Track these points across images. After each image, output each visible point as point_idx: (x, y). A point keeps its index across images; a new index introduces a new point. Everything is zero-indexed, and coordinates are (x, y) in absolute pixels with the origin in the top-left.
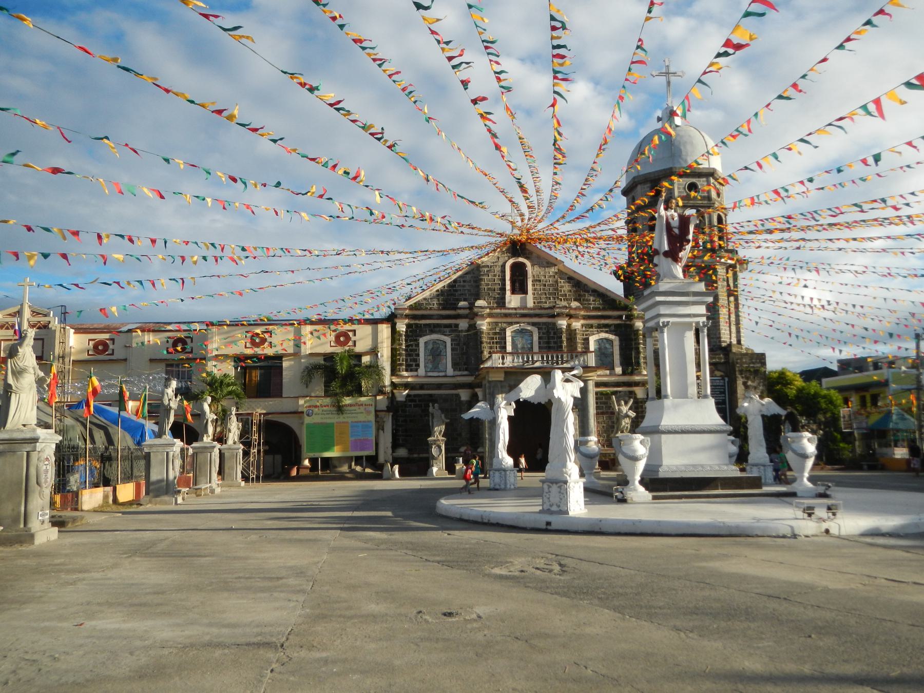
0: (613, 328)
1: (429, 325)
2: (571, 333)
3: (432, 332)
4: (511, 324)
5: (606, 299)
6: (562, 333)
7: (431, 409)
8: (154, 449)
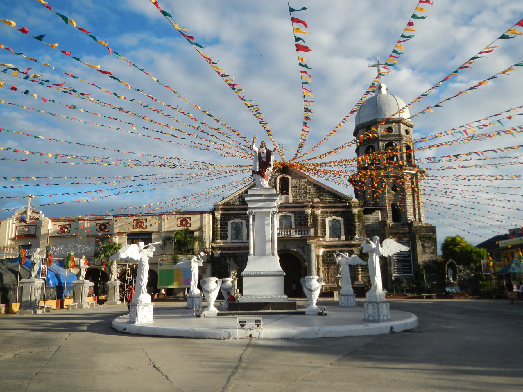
0: (340, 213)
1: (233, 214)
2: (314, 217)
3: (235, 218)
5: (337, 197)
6: (308, 216)
7: (228, 261)
8: (25, 285)
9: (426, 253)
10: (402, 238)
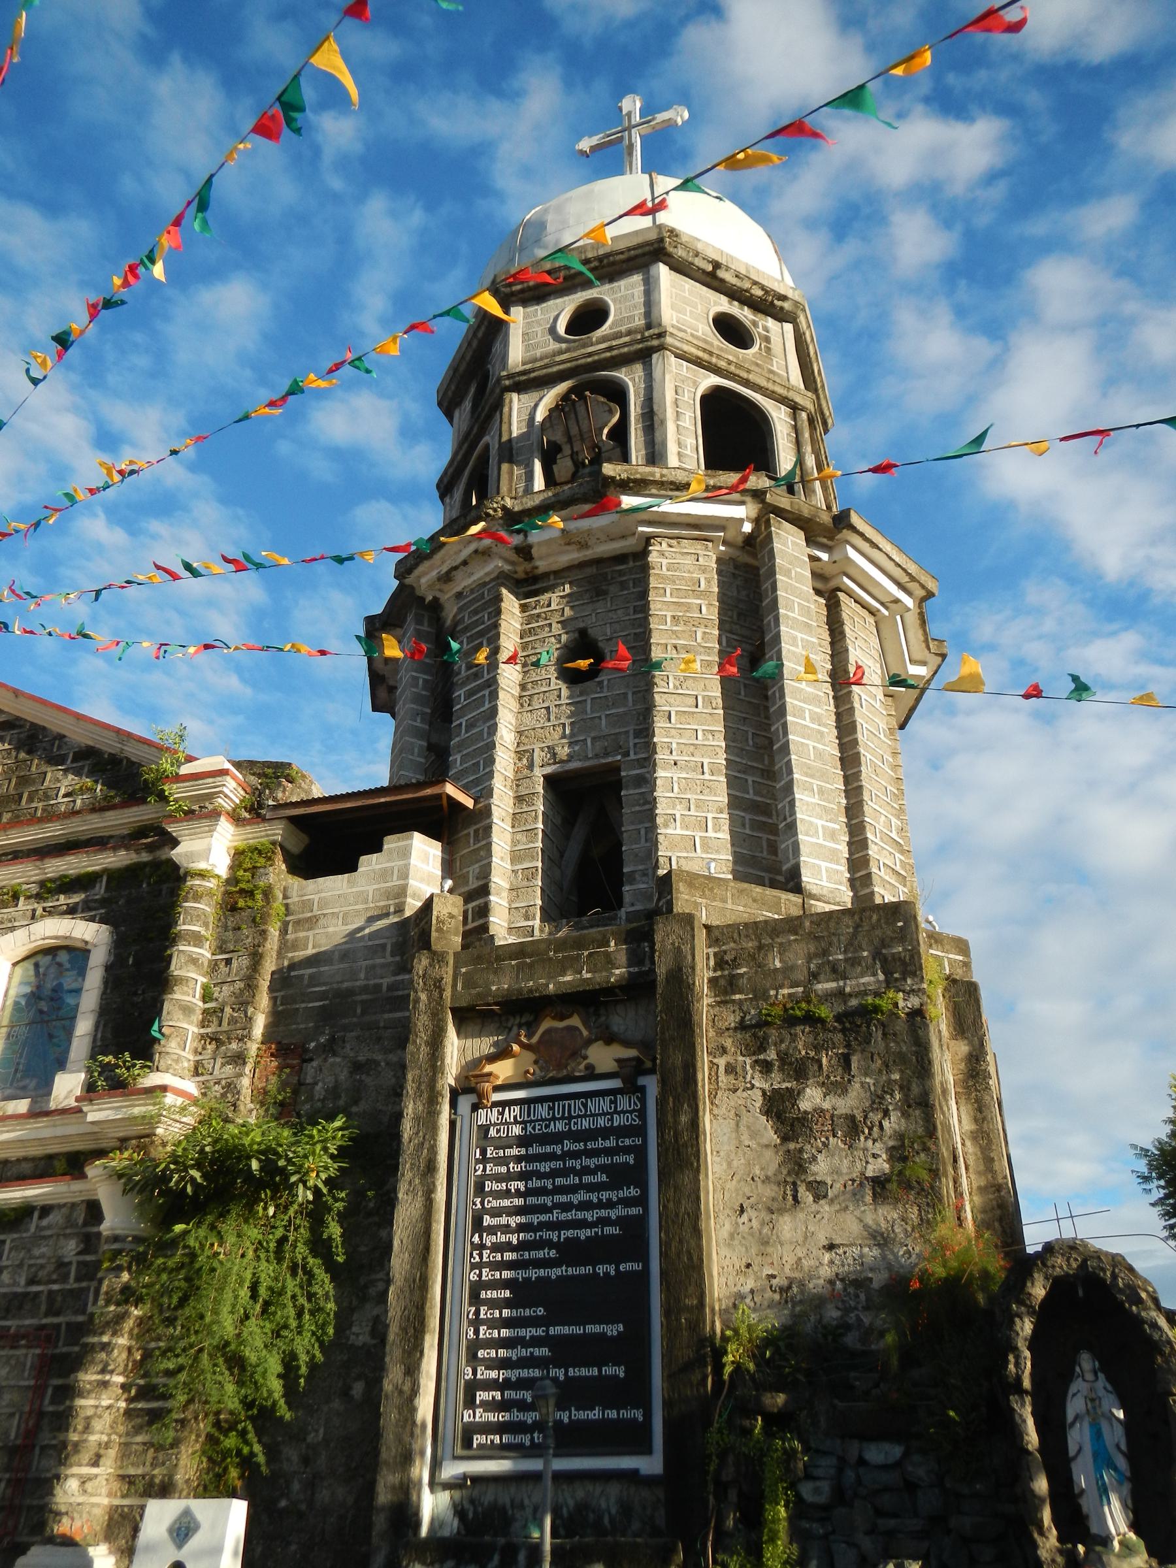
0: (100, 890)
9: (819, 1190)
10: (577, 1054)
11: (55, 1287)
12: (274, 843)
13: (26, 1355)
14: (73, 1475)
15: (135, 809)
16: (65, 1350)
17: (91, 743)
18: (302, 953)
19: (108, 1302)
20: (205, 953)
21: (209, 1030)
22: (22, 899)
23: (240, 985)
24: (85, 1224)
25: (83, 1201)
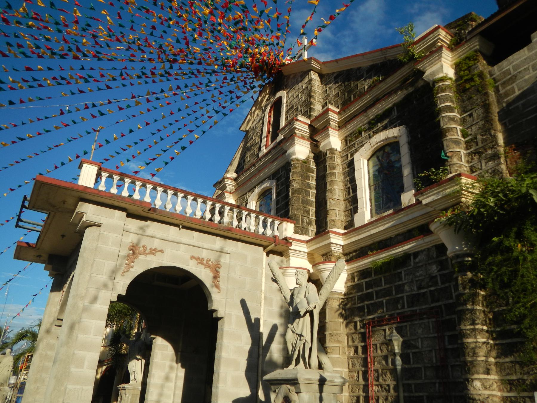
4: (251, 190)
11: (432, 289)
12: (476, 51)
13: (428, 322)
14: (476, 379)
15: (399, 72)
16: (447, 317)
17: (371, 63)
18: (512, 96)
19: (464, 288)
20: (456, 114)
21: (472, 150)
22: (363, 133)
23: (481, 123)
24: (437, 257)
25: (432, 246)
